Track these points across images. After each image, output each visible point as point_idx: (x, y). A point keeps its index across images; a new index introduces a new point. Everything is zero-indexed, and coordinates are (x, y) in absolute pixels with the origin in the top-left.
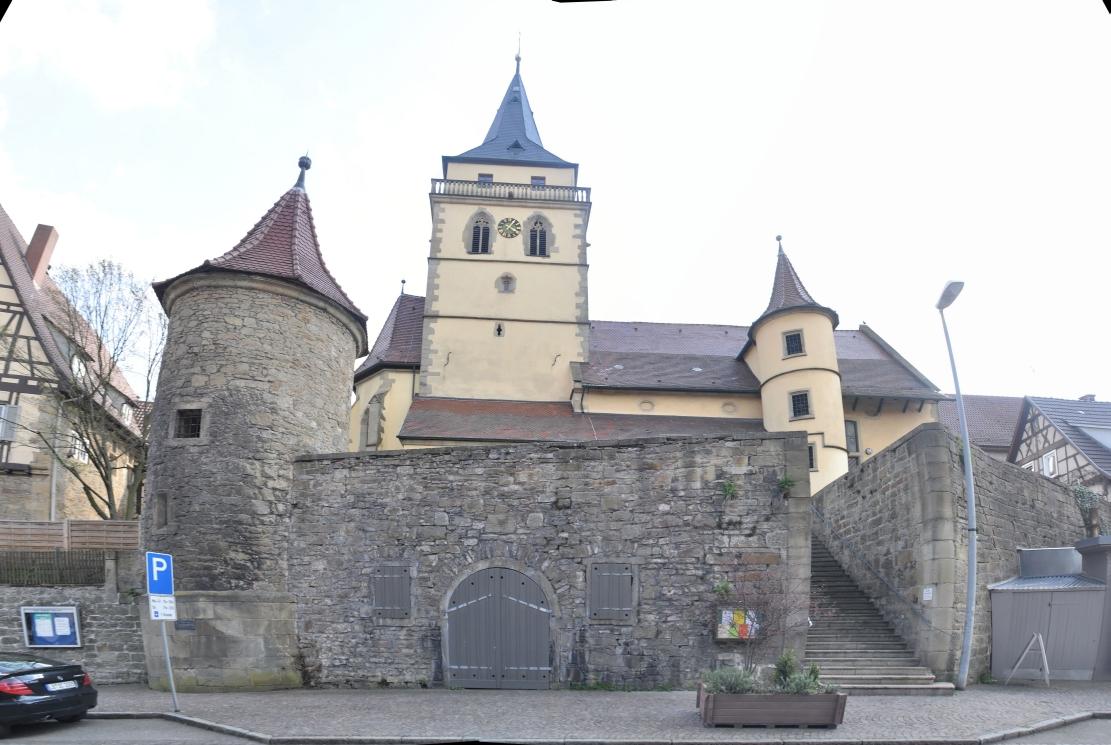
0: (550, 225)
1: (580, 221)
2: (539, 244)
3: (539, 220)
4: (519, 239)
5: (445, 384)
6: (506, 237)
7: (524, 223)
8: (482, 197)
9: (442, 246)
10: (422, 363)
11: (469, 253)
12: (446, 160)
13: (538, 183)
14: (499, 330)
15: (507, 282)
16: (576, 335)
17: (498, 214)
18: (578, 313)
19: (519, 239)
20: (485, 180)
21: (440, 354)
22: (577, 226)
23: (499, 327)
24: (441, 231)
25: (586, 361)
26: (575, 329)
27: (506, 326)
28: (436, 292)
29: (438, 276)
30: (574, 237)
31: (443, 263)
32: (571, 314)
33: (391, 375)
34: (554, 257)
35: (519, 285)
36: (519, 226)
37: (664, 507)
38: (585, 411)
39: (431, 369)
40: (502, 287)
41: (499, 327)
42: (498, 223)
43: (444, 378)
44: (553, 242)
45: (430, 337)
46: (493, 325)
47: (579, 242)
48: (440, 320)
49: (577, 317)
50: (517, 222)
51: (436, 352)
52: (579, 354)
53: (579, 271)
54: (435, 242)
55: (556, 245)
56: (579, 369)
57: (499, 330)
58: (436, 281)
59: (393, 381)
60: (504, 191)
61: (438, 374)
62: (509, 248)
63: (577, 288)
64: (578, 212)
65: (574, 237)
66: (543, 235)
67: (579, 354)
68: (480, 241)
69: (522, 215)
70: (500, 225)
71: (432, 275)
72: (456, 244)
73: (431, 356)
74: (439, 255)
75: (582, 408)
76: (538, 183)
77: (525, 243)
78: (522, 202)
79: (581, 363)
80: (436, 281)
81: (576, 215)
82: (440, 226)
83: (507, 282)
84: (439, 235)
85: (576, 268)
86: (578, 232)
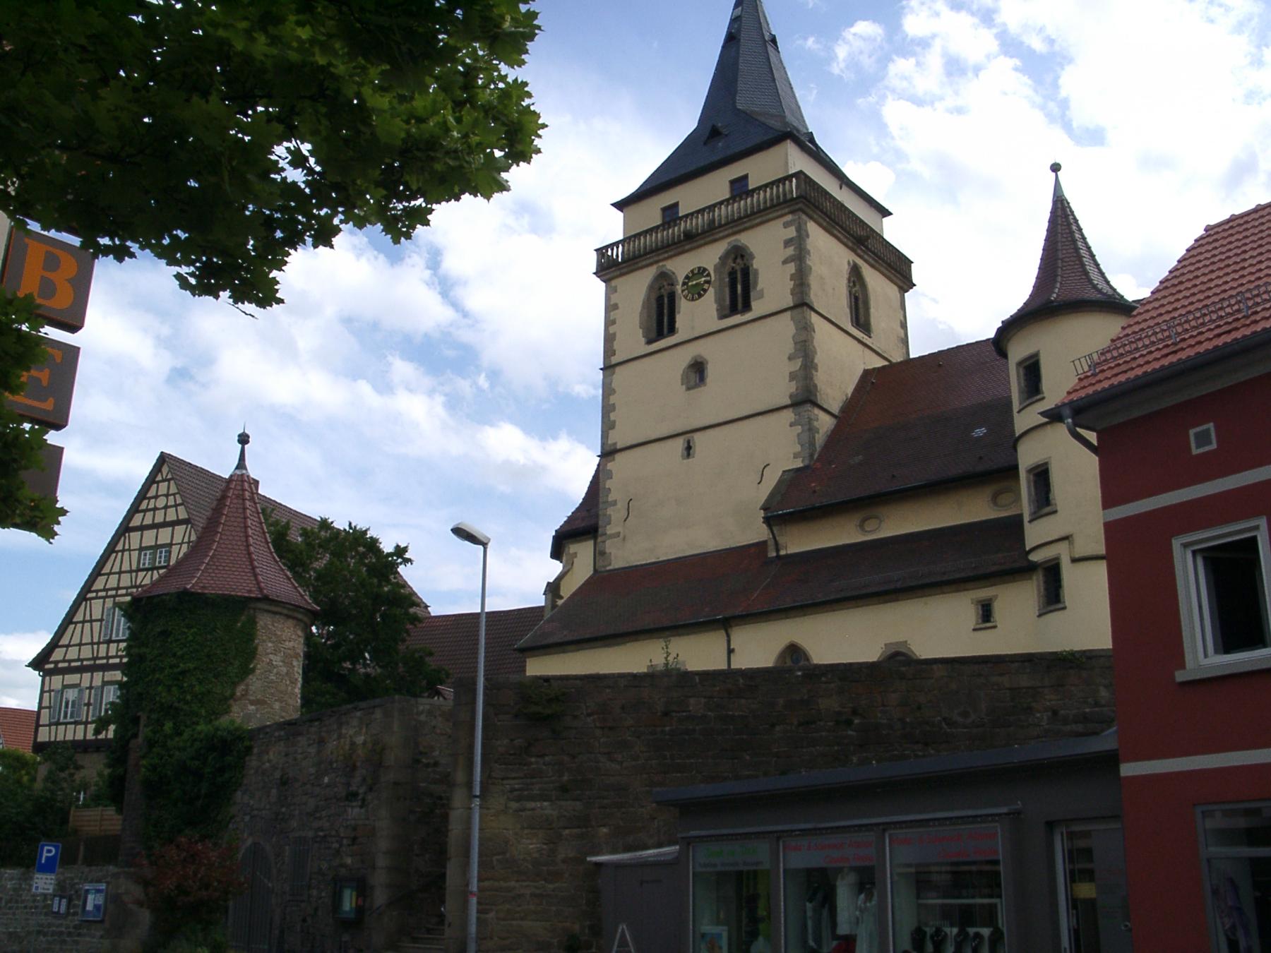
0: (752, 256)
1: (791, 232)
2: (738, 291)
3: (739, 255)
4: (711, 294)
5: (632, 547)
6: (693, 300)
7: (716, 268)
8: (674, 243)
9: (616, 345)
10: (600, 523)
11: (649, 342)
12: (620, 205)
13: (740, 187)
14: (689, 448)
15: (698, 370)
16: (791, 425)
17: (681, 266)
18: (792, 387)
19: (711, 294)
20: (670, 213)
21: (619, 506)
22: (787, 243)
23: (689, 442)
24: (614, 322)
25: (807, 462)
26: (789, 415)
27: (698, 438)
28: (613, 416)
29: (614, 391)
30: (785, 262)
31: (618, 369)
32: (783, 391)
33: (573, 548)
34: (758, 308)
35: (711, 371)
36: (709, 275)
37: (326, 780)
38: (782, 553)
39: (610, 530)
40: (694, 377)
41: (689, 442)
42: (681, 279)
43: (624, 539)
44: (756, 283)
45: (609, 484)
46: (679, 443)
47: (791, 268)
48: (618, 457)
49: (791, 396)
50: (705, 270)
51: (615, 503)
52: (796, 456)
53: (792, 319)
54: (609, 339)
55: (759, 288)
56: (792, 480)
57: (689, 448)
58: (613, 399)
59: (575, 555)
60: (700, 221)
61: (618, 534)
62: (697, 314)
63: (789, 347)
64: (789, 217)
65: (785, 262)
66: (746, 272)
67: (796, 456)
68: (661, 319)
69: (709, 257)
70: (684, 284)
71: (608, 390)
72: (633, 340)
73: (609, 511)
74: (614, 360)
75: (778, 550)
76: (740, 187)
77: (719, 301)
78: (710, 233)
79: (798, 470)
80: (613, 399)
81: (786, 225)
82: (613, 315)
83: (698, 370)
84: (611, 330)
85: (788, 314)
86: (791, 251)
